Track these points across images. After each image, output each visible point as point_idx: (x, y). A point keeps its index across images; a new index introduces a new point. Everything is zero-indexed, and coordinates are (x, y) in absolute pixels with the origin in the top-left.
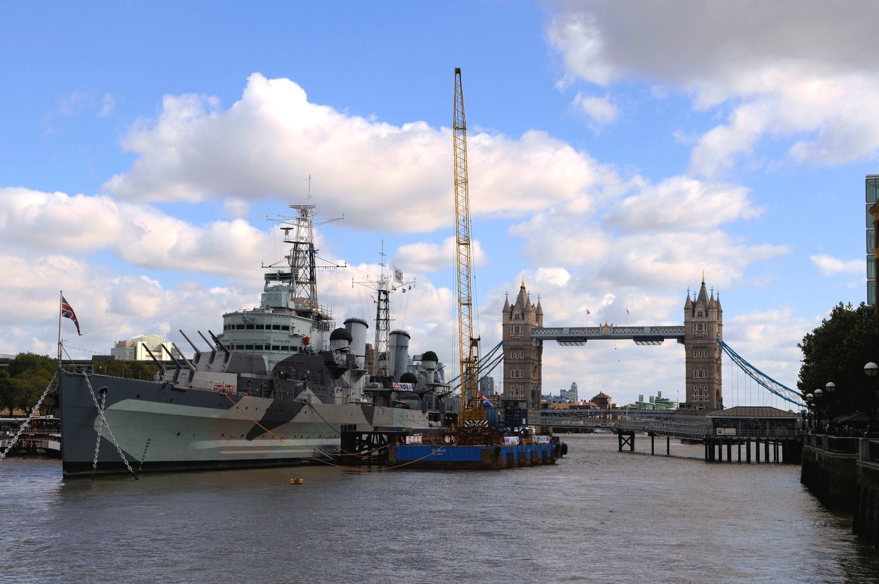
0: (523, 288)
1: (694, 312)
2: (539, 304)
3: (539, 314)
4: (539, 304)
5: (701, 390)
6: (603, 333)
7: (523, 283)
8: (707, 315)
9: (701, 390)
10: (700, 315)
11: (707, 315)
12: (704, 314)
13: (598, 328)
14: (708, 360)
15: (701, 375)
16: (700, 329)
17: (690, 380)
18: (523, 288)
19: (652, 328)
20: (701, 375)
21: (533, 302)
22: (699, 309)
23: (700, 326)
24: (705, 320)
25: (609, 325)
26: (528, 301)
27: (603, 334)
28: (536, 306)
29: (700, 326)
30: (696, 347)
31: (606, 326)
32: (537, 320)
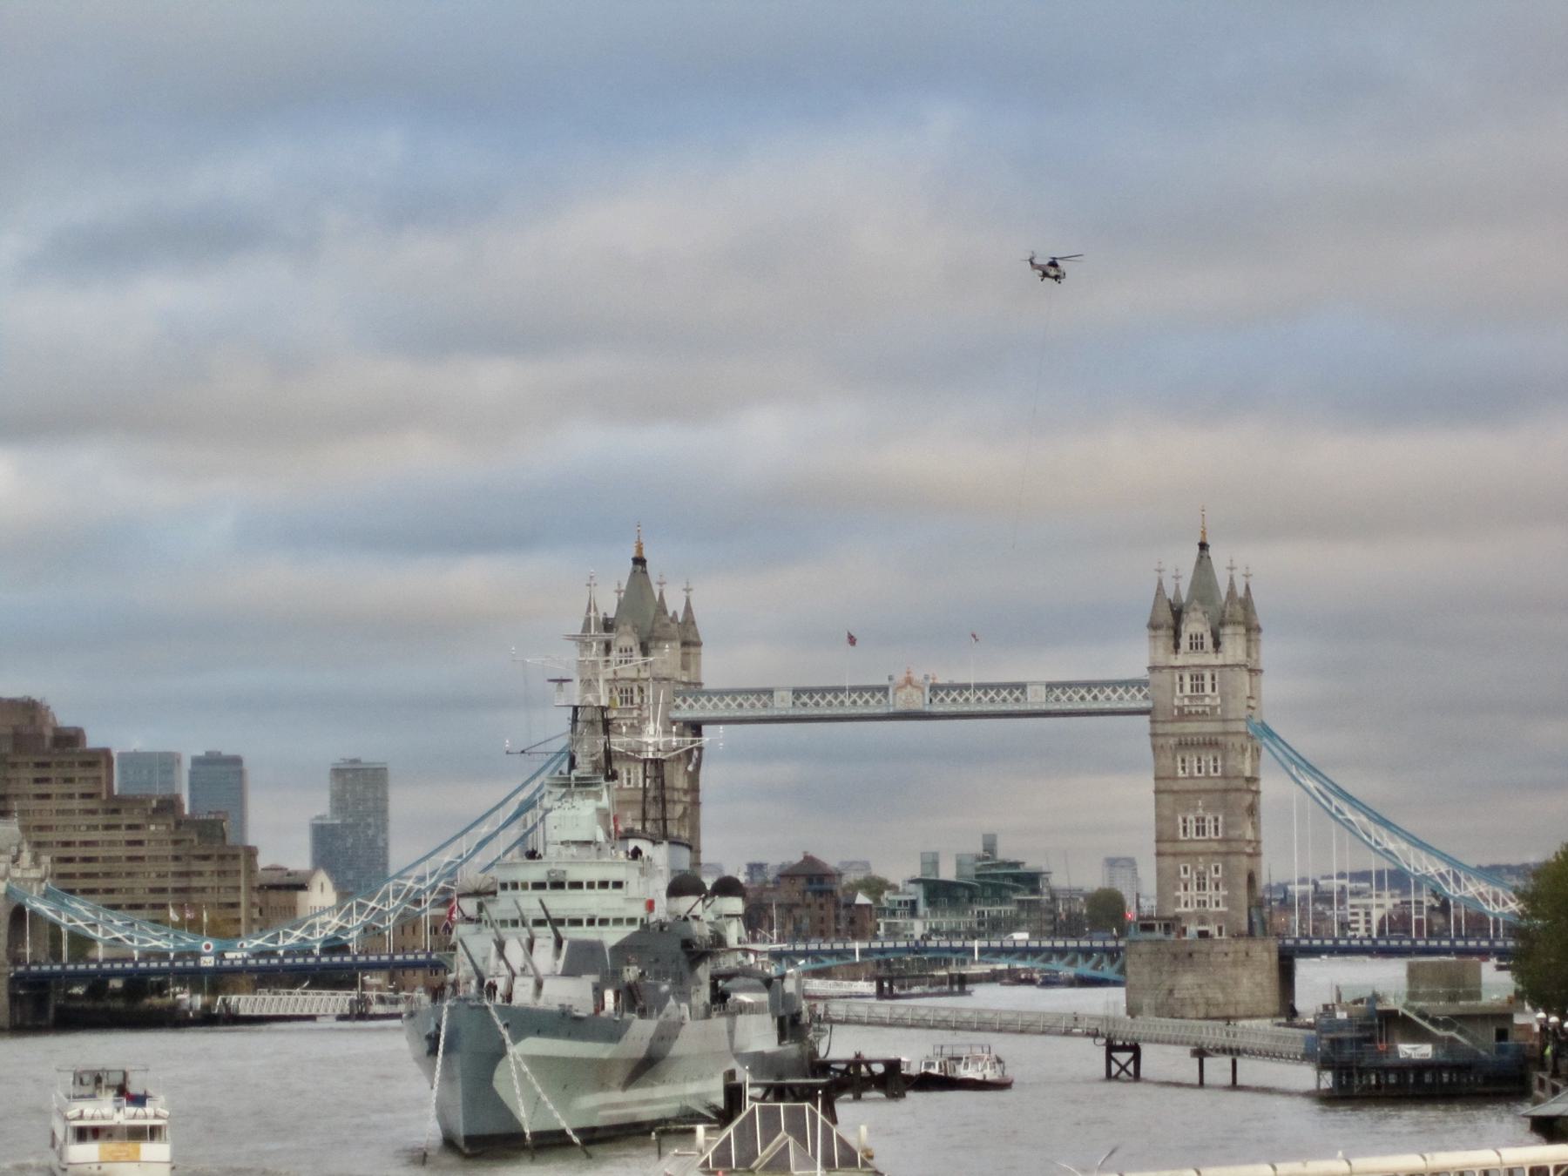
0: (639, 561)
1: (1177, 635)
2: (688, 609)
3: (690, 643)
4: (688, 609)
5: (1201, 877)
6: (899, 702)
7: (640, 548)
8: (1217, 644)
9: (1201, 877)
10: (1197, 644)
11: (1217, 644)
12: (1208, 641)
13: (884, 690)
14: (1221, 784)
15: (1201, 830)
16: (1198, 687)
17: (1167, 847)
18: (639, 561)
19: (1050, 686)
20: (1201, 830)
21: (675, 605)
22: (1194, 625)
23: (1198, 679)
24: (1212, 659)
25: (918, 677)
26: (661, 607)
27: (900, 706)
28: (680, 618)
29: (1198, 679)
30: (1184, 745)
31: (909, 681)
32: (685, 667)
